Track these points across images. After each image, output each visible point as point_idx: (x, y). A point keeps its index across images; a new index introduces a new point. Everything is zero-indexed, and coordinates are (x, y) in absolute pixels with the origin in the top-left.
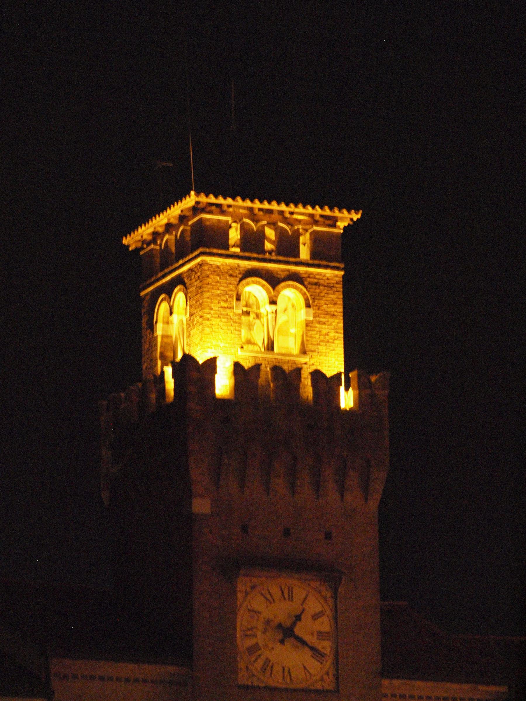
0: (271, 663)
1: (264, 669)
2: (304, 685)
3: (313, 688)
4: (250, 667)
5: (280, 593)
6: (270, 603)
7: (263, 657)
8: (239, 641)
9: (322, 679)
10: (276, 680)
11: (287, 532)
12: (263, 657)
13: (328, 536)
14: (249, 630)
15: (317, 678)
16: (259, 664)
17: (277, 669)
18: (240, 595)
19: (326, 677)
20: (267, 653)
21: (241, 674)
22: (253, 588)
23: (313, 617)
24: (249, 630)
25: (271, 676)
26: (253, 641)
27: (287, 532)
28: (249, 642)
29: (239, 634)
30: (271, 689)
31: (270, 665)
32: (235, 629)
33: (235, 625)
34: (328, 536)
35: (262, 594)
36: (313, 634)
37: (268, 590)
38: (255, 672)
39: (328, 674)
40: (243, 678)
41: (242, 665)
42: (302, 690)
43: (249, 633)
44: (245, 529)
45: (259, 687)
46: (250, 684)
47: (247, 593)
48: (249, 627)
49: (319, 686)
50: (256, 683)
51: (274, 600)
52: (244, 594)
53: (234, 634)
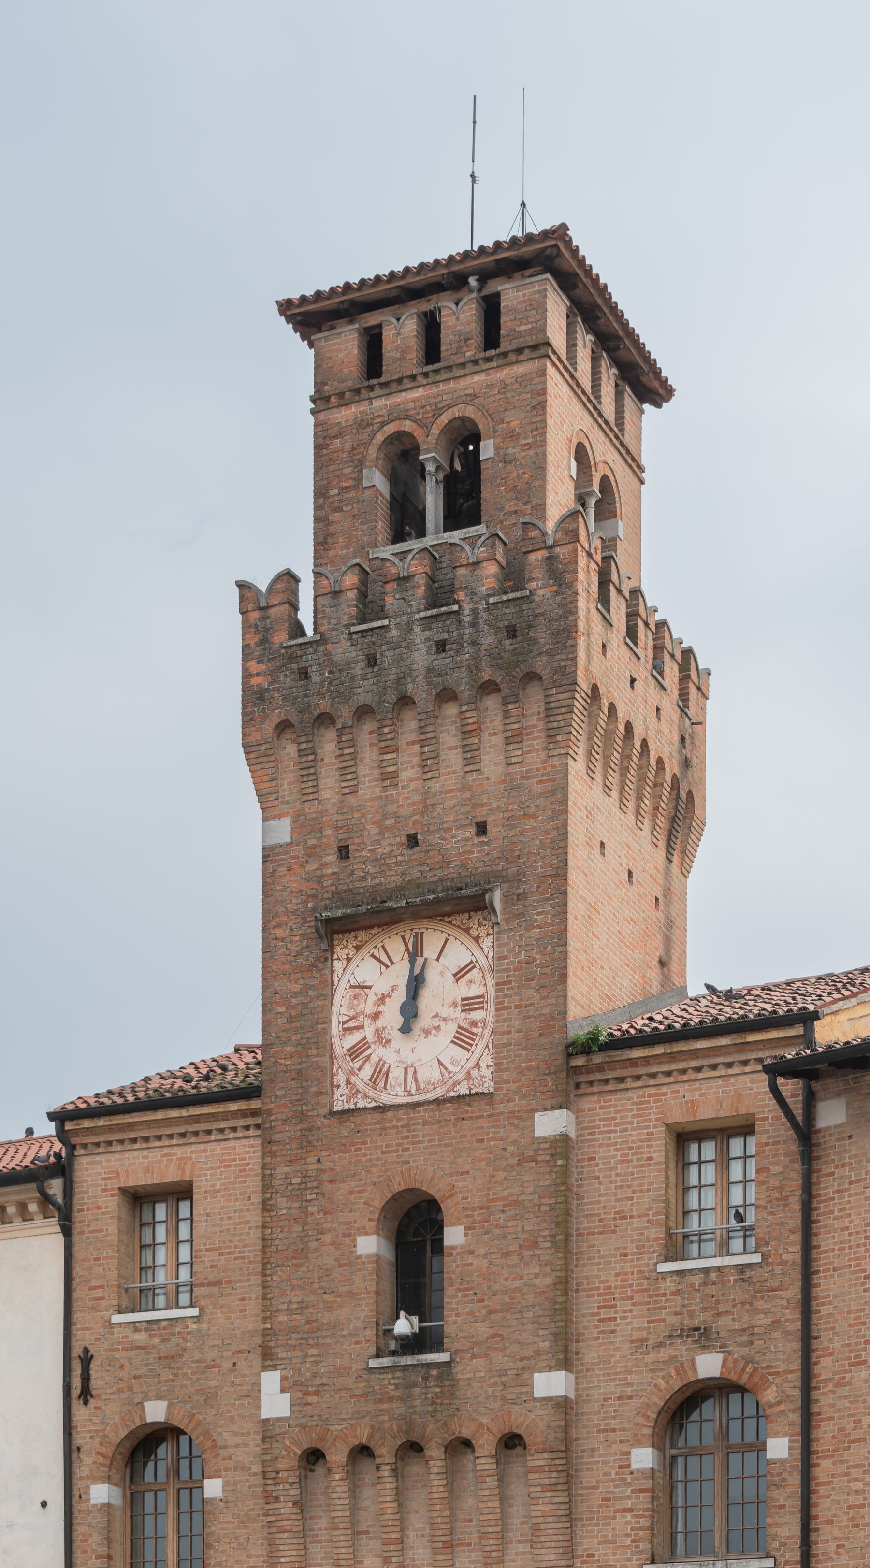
0: (386, 1066)
1: (374, 1079)
2: (438, 1093)
3: (452, 1094)
4: (353, 1079)
5: (403, 947)
6: (387, 967)
7: (374, 1059)
8: (336, 1042)
9: (468, 1077)
10: (394, 1094)
11: (413, 841)
12: (374, 1059)
13: (482, 829)
14: (352, 1018)
15: (460, 1076)
16: (367, 1072)
17: (396, 1074)
18: (338, 966)
19: (474, 1073)
20: (378, 1052)
21: (338, 1092)
22: (358, 948)
23: (455, 975)
24: (352, 1018)
25: (385, 1087)
26: (355, 1037)
27: (413, 841)
28: (352, 1039)
29: (335, 1029)
30: (382, 1109)
31: (385, 1069)
32: (327, 1022)
33: (329, 1017)
34: (482, 829)
35: (373, 956)
36: (455, 1005)
37: (383, 947)
38: (361, 1086)
39: (477, 1065)
40: (341, 1101)
41: (341, 1078)
42: (438, 1102)
43: (351, 1024)
44: (344, 852)
45: (365, 1109)
46: (352, 1107)
47: (349, 960)
48: (352, 1013)
49: (463, 1090)
50: (361, 1103)
51: (392, 963)
52: (345, 962)
53: (326, 1032)
